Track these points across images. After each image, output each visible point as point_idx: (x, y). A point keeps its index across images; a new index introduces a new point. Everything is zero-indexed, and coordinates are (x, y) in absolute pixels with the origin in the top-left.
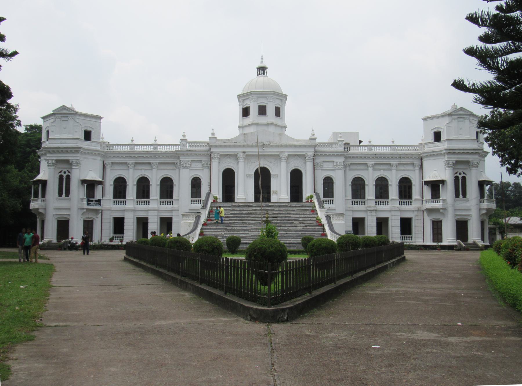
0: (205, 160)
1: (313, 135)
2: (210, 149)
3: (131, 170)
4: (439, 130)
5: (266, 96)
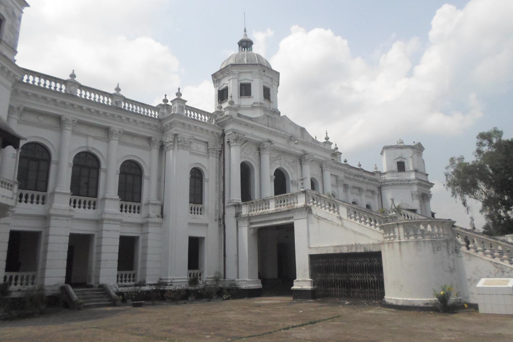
1: (327, 138)
3: (68, 133)
4: (403, 160)
5: (271, 76)
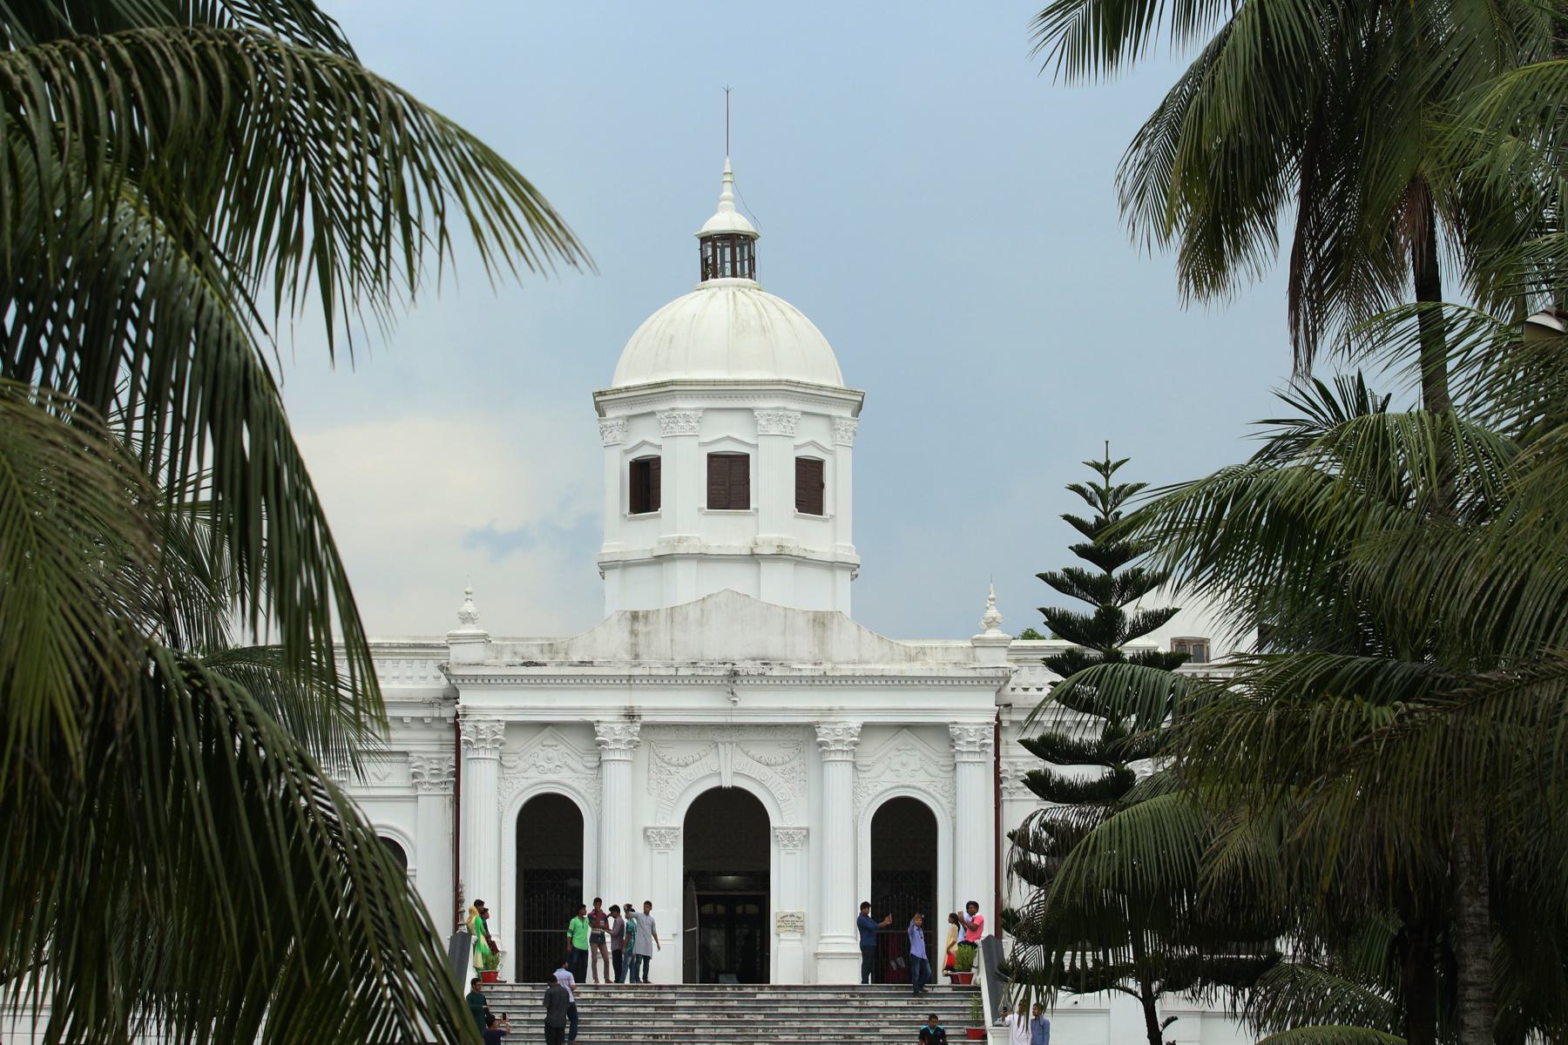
2: (451, 697)
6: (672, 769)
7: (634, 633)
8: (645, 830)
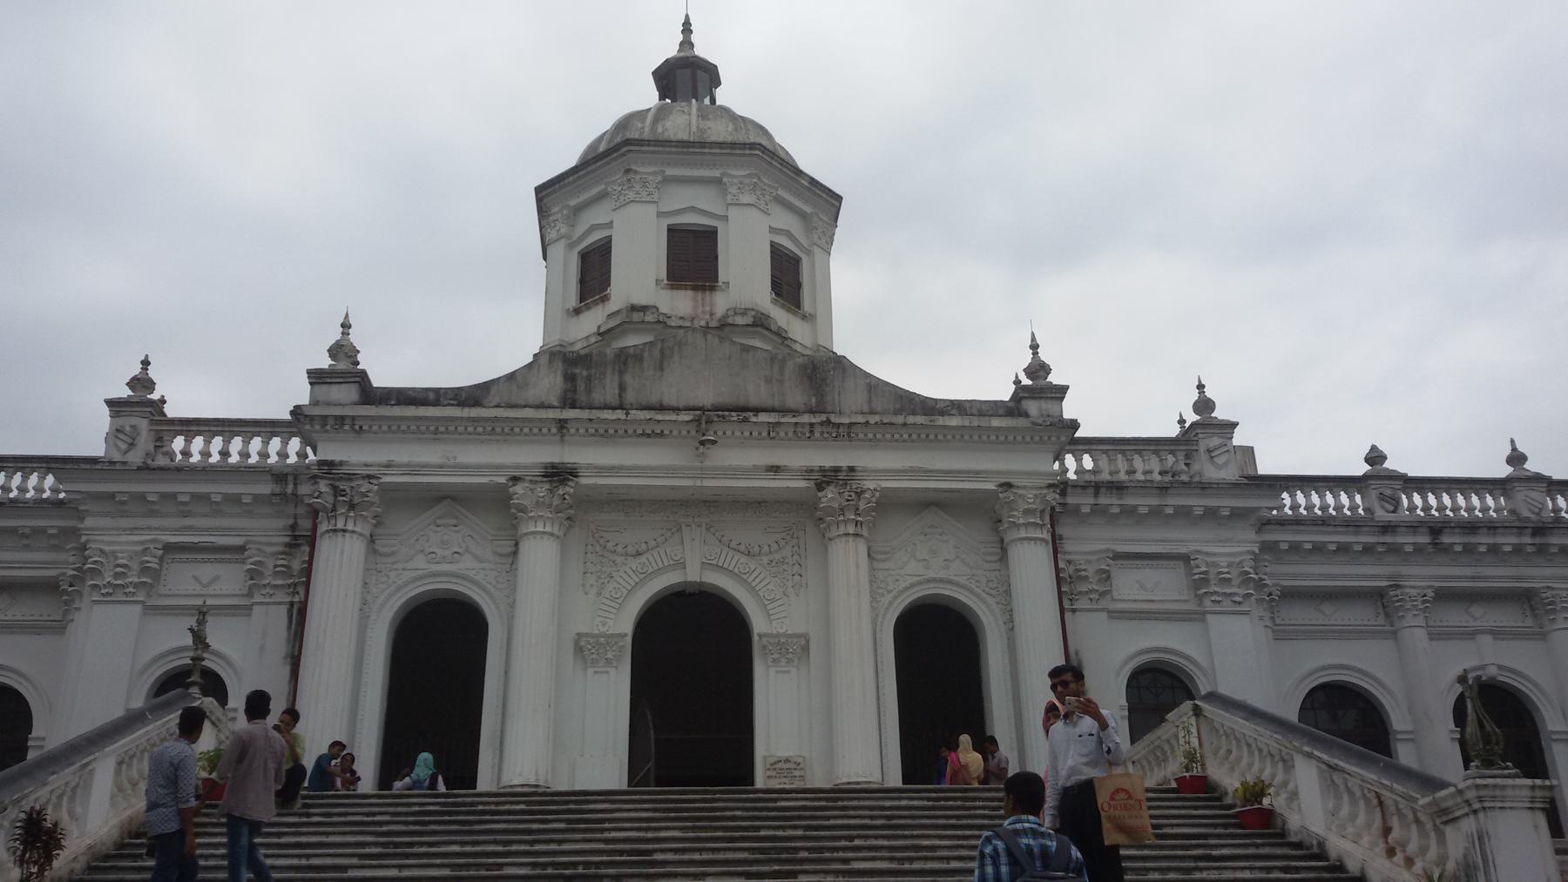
0: (267, 532)
1: (1038, 369)
5: (716, 173)
6: (619, 560)
7: (570, 378)
8: (576, 643)
